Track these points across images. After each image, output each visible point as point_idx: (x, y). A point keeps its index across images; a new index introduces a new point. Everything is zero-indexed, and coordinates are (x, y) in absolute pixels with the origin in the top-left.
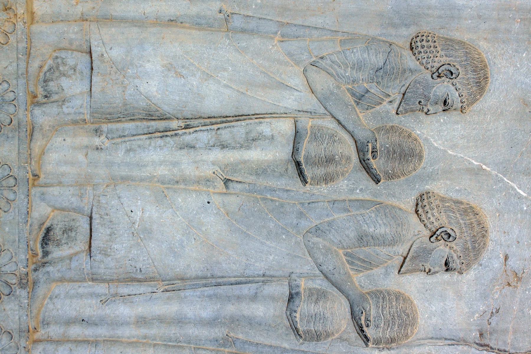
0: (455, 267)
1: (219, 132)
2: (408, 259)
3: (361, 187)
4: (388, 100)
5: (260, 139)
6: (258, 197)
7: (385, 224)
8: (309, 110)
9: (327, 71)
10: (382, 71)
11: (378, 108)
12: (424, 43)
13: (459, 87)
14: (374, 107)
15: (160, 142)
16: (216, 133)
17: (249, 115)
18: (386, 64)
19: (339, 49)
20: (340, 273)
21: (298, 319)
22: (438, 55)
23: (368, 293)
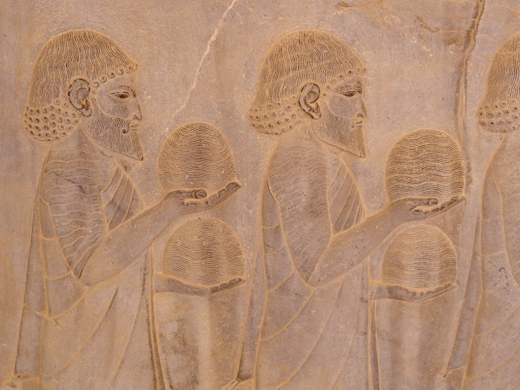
0: (355, 83)
3: (245, 207)
4: (123, 172)
5: (183, 336)
6: (260, 339)
7: (295, 182)
8: (142, 277)
11: (134, 185)
12: (41, 125)
13: (100, 78)
14: (134, 190)
17: (152, 352)
18: (74, 180)
19: (55, 240)
20: (363, 240)
21: (425, 290)
22: (56, 107)
23: (391, 199)
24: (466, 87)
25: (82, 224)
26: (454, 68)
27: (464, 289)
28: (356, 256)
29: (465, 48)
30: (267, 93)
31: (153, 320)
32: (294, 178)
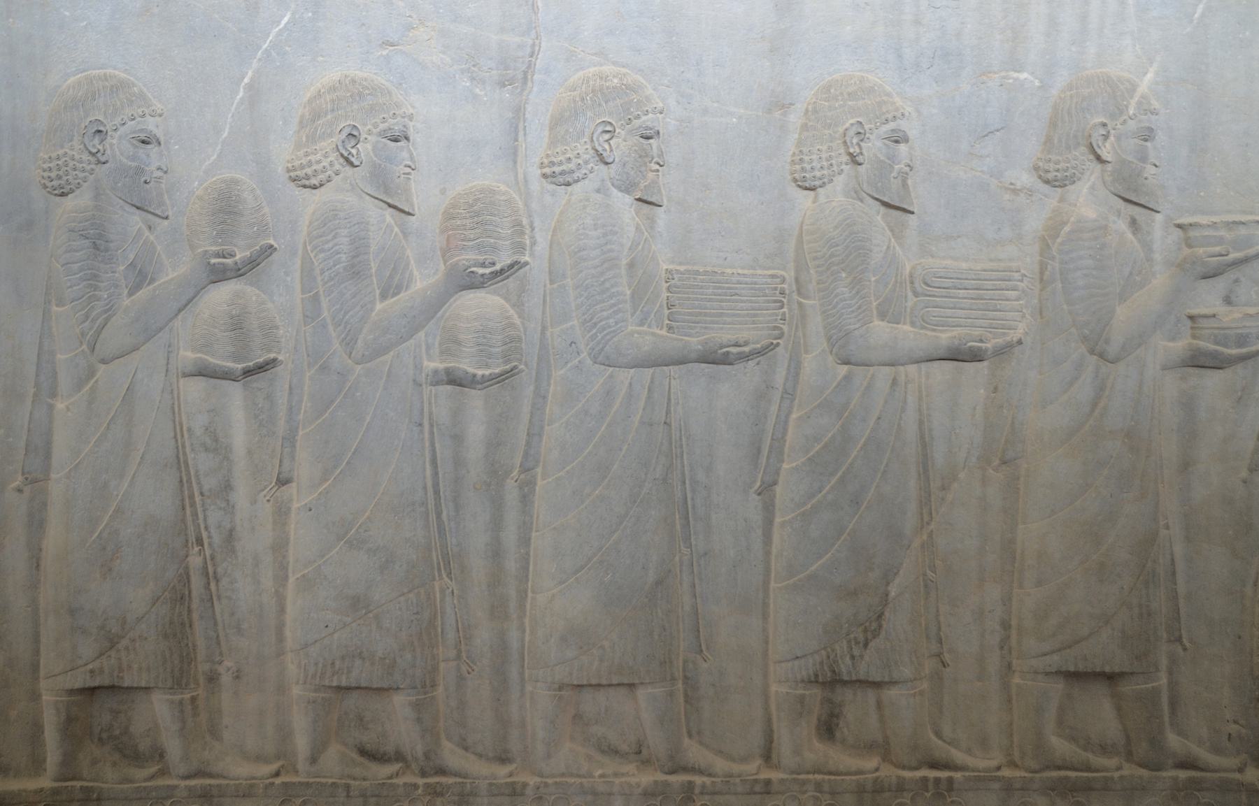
1: (207, 494)
2: (389, 201)
5: (215, 430)
6: (301, 433)
7: (335, 237)
8: (166, 355)
9: (102, 326)
10: (98, 242)
14: (159, 254)
15: (224, 582)
16: (209, 497)
17: (177, 448)
18: (87, 236)
21: (487, 372)
23: (445, 263)
24: (525, 135)
25: (96, 288)
26: (510, 113)
27: (534, 373)
28: (405, 327)
29: (523, 90)
30: (304, 139)
31: (180, 409)
32: (333, 233)
